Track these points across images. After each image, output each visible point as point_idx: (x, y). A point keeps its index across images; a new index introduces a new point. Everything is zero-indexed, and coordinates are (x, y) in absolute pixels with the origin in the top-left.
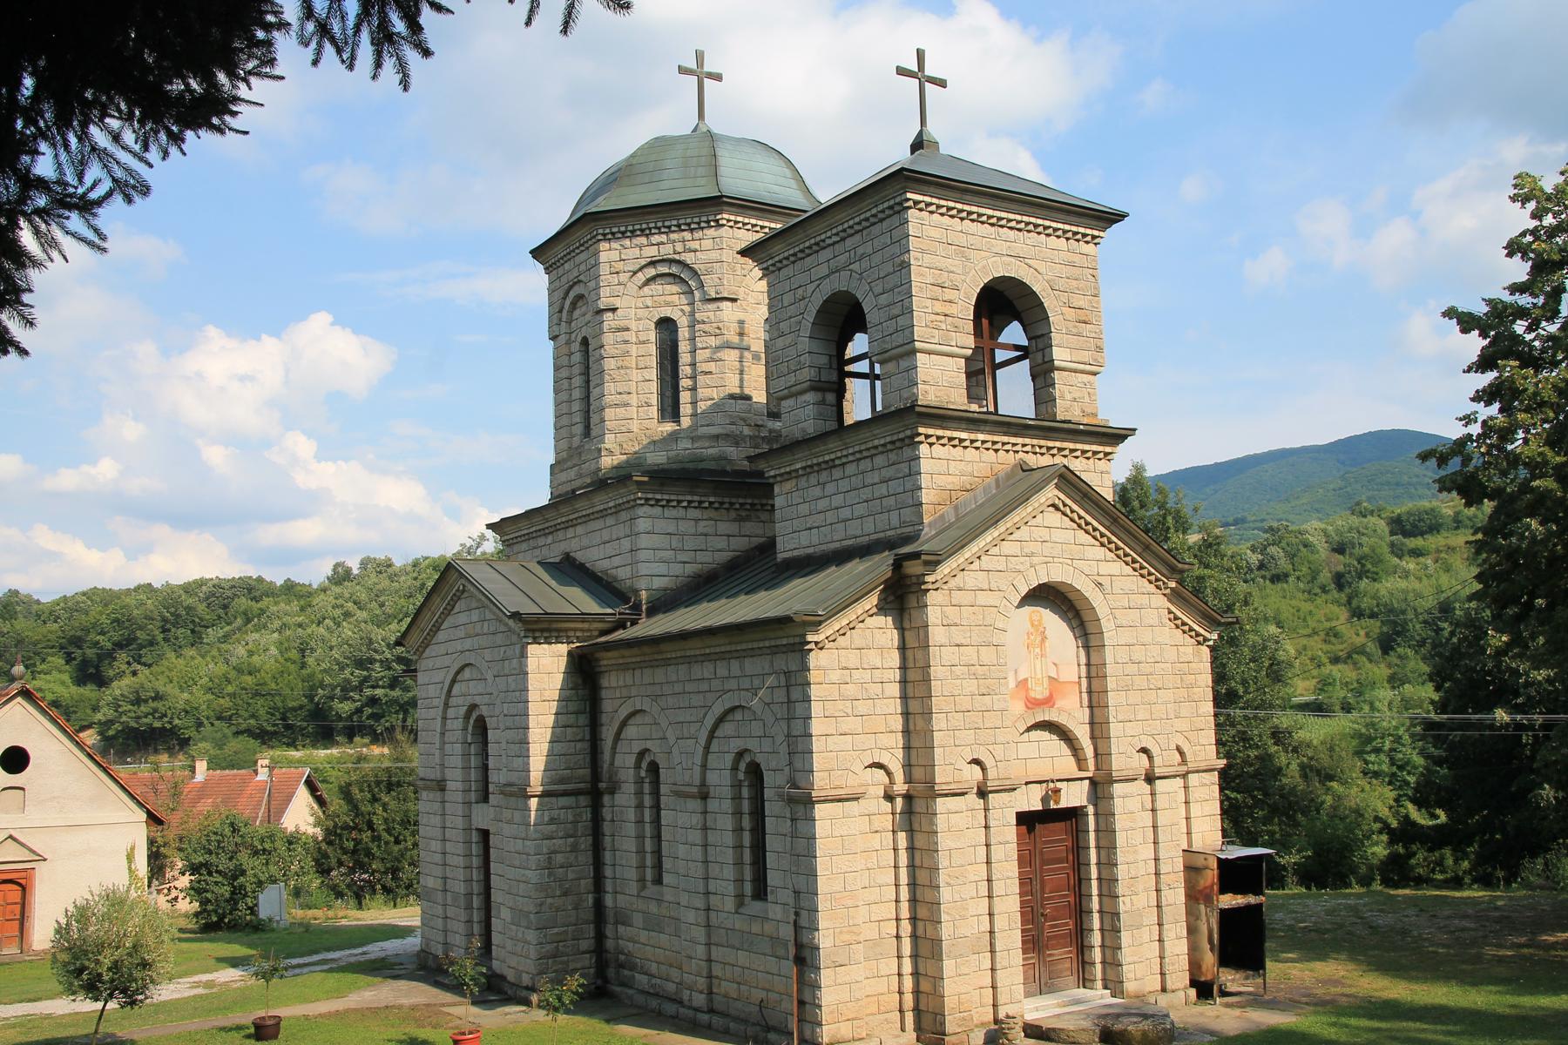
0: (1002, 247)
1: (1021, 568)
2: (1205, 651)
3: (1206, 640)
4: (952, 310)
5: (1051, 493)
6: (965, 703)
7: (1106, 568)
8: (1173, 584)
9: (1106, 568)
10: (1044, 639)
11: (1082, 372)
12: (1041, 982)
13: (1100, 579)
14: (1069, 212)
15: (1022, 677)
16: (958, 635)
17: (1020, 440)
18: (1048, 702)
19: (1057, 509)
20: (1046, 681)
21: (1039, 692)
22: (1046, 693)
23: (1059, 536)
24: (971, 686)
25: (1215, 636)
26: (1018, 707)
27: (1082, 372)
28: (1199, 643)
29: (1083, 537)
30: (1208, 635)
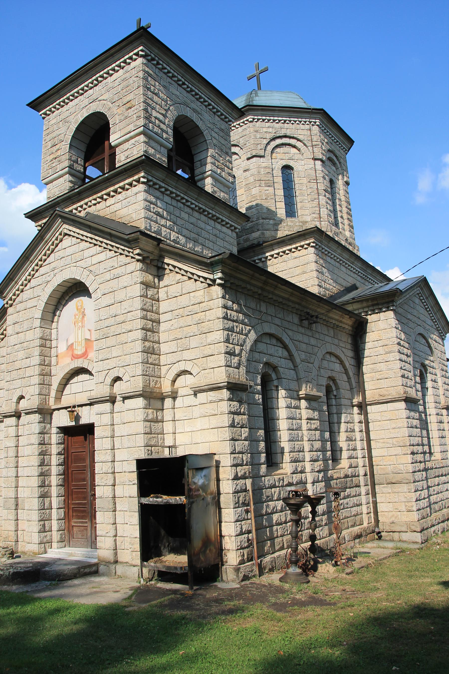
0: (86, 102)
1: (49, 279)
2: (217, 291)
3: (214, 281)
4: (59, 153)
5: (66, 228)
6: (17, 365)
7: (95, 260)
8: (138, 251)
9: (95, 260)
10: (84, 315)
11: (132, 138)
12: (68, 538)
13: (91, 268)
14: (112, 55)
15: (70, 343)
16: (17, 328)
17: (82, 203)
18: (85, 355)
19: (70, 235)
20: (83, 342)
21: (79, 351)
22: (84, 350)
23: (69, 251)
24: (21, 354)
25: (220, 275)
26: (68, 360)
27: (132, 138)
28: (209, 285)
29: (84, 245)
30: (211, 276)
